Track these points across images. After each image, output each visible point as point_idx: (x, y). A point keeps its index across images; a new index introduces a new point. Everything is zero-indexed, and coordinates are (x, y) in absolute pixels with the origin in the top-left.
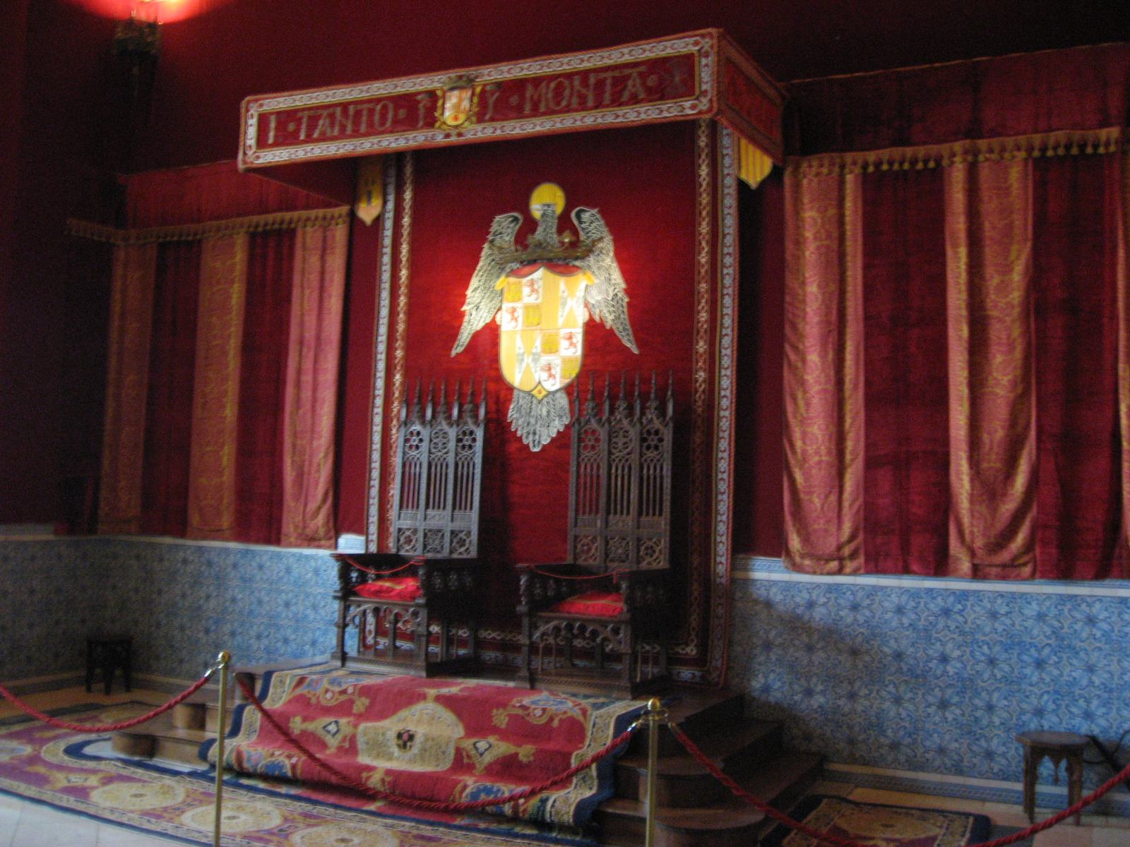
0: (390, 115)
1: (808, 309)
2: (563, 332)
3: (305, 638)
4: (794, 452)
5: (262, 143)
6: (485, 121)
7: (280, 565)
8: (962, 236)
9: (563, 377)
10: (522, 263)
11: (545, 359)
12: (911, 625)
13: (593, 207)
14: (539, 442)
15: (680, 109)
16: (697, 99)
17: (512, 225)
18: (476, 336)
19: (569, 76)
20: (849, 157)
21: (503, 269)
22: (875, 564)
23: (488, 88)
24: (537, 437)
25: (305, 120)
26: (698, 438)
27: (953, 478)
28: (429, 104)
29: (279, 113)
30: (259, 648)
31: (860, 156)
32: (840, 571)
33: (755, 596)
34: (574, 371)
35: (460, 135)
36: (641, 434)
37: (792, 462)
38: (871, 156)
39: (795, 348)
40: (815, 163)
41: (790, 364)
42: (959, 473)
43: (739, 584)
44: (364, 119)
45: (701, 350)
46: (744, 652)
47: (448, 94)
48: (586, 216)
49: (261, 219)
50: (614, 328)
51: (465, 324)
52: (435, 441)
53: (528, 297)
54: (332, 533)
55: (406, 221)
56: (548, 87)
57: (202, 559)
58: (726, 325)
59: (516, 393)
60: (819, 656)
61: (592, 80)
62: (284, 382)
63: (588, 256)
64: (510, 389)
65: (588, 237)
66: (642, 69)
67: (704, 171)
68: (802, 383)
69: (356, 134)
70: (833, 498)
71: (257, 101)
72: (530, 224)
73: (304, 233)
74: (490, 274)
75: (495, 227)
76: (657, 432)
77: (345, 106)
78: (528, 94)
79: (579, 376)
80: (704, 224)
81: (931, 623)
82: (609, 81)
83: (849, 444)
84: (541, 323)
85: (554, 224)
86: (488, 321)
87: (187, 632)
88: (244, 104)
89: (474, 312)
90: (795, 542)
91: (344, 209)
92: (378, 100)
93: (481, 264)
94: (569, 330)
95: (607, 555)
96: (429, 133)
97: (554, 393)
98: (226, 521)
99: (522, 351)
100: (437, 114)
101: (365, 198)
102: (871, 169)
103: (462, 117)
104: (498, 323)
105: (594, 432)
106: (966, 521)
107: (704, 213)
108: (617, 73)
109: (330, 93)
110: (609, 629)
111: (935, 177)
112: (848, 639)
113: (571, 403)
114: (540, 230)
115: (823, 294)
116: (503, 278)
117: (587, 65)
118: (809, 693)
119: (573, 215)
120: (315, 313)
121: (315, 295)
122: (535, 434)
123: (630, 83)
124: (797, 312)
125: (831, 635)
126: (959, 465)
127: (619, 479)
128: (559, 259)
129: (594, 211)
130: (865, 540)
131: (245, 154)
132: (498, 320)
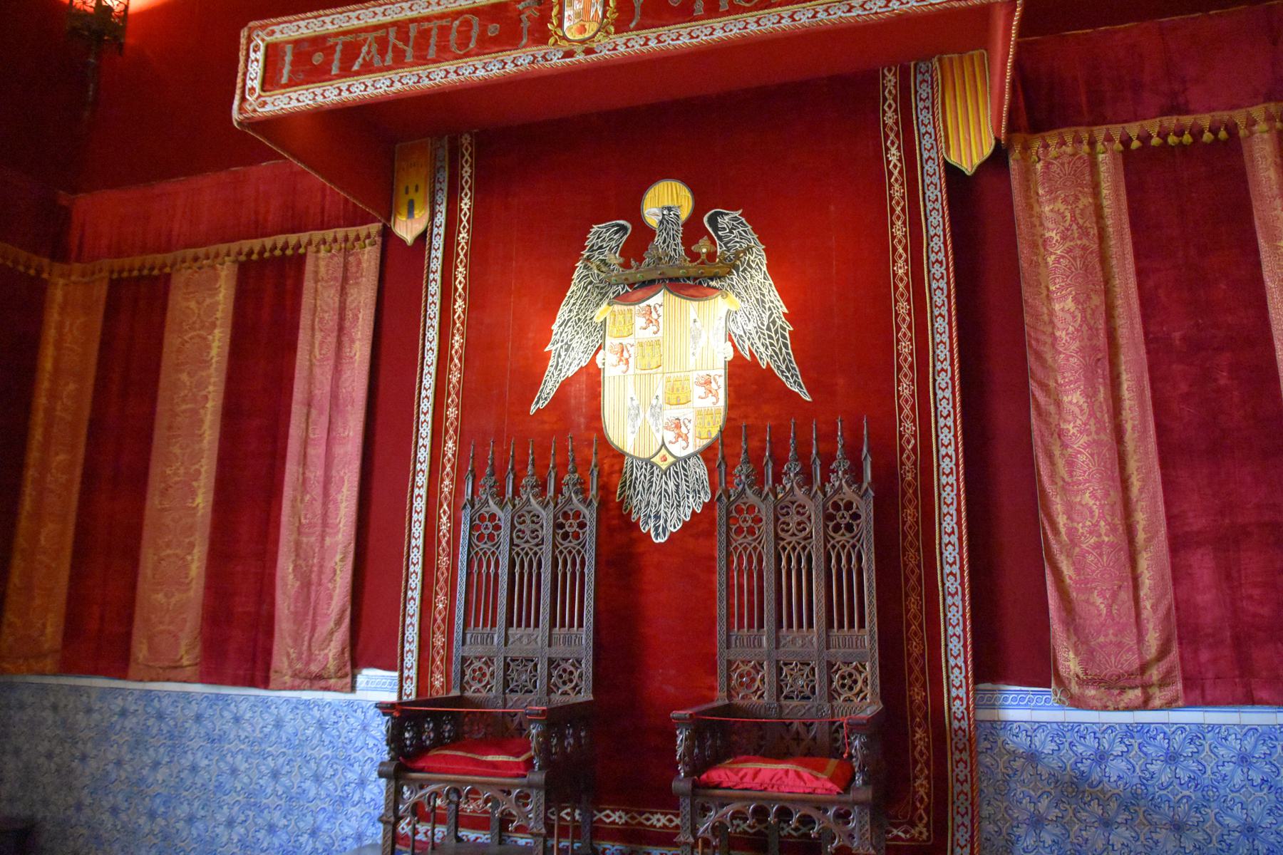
0: (475, 33)
1: (1058, 334)
3: (301, 824)
4: (1056, 532)
5: (269, 82)
7: (266, 716)
10: (631, 286)
11: (671, 413)
14: (664, 529)
20: (1100, 132)
24: (662, 522)
26: (910, 514)
30: (230, 839)
31: (1116, 130)
32: (1145, 705)
33: (1011, 747)
35: (589, 51)
36: (825, 509)
37: (1055, 547)
38: (1134, 129)
39: (1044, 386)
40: (1053, 142)
41: (1038, 406)
45: (906, 393)
46: (999, 833)
48: (724, 221)
49: (256, 244)
54: (348, 668)
55: (463, 236)
57: (149, 709)
59: (627, 460)
62: (284, 457)
63: (730, 273)
64: (620, 455)
67: (894, 155)
68: (1061, 434)
69: (421, 60)
70: (1125, 596)
71: (263, 28)
72: (641, 238)
73: (317, 259)
74: (586, 301)
75: (591, 239)
76: (849, 505)
83: (1141, 518)
84: (664, 365)
86: (583, 364)
87: (123, 816)
88: (244, 33)
89: (563, 354)
90: (1069, 662)
91: (374, 228)
94: (703, 373)
95: (780, 690)
96: (539, 51)
97: (686, 459)
98: (188, 654)
99: (635, 403)
101: (404, 210)
103: (592, 28)
104: (600, 366)
105: (751, 509)
110: (831, 813)
112: (1165, 806)
114: (658, 240)
115: (1084, 311)
116: (604, 305)
119: (705, 219)
120: (332, 362)
121: (332, 339)
122: (657, 517)
124: (1043, 338)
125: (1136, 803)
128: (689, 278)
129: (737, 214)
130: (1182, 658)
131: (243, 99)
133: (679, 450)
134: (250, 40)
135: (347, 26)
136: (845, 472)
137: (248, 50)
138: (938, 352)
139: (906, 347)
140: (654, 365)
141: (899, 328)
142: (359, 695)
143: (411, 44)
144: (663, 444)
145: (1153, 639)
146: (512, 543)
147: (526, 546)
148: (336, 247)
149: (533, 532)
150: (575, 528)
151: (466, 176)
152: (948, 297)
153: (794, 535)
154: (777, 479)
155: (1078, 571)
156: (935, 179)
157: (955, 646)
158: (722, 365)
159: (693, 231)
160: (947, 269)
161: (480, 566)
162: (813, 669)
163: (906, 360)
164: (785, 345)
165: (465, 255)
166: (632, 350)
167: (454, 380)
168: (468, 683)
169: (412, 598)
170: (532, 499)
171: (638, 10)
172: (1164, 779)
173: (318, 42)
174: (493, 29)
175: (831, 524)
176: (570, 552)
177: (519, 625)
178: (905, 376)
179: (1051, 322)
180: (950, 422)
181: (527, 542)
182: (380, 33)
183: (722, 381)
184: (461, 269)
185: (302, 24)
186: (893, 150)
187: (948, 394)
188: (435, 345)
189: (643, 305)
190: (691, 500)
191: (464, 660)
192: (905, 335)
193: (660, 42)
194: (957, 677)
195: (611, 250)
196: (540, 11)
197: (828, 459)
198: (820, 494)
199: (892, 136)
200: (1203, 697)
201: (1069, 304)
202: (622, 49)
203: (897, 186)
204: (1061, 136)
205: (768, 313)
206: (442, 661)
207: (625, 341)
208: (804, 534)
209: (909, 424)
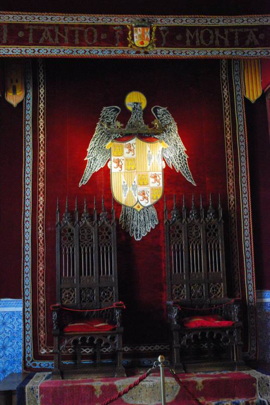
0: (96, 35)
9: (152, 198)
11: (140, 189)
13: (165, 107)
18: (95, 174)
19: (213, 28)
21: (109, 138)
23: (161, 29)
25: (31, 31)
28: (122, 33)
29: (9, 25)
34: (159, 196)
43: (262, 305)
44: (77, 36)
45: (231, 184)
47: (134, 29)
48: (161, 111)
50: (181, 172)
51: (87, 168)
53: (126, 154)
55: (42, 106)
56: (199, 33)
58: (243, 171)
59: (123, 207)
61: (226, 32)
63: (163, 133)
64: (119, 205)
65: (162, 123)
66: (255, 30)
67: (225, 92)
69: (72, 43)
75: (103, 113)
77: (61, 27)
78: (187, 35)
82: (236, 34)
84: (138, 170)
85: (140, 113)
89: (93, 162)
92: (87, 26)
93: (96, 134)
94: (154, 173)
95: (191, 295)
96: (126, 49)
97: (148, 207)
99: (125, 184)
100: (129, 39)
101: (11, 90)
103: (146, 43)
108: (241, 30)
109: (49, 17)
110: (227, 332)
113: (158, 213)
114: (133, 116)
116: (110, 142)
117: (221, 24)
119: (152, 110)
122: (137, 230)
123: (249, 37)
129: (165, 109)
133: (145, 203)
135: (34, 22)
136: (213, 214)
138: (242, 169)
139: (231, 167)
140: (133, 169)
141: (228, 160)
143: (66, 35)
144: (138, 201)
146: (79, 241)
147: (86, 242)
149: (88, 236)
150: (107, 234)
151: (42, 78)
152: (246, 149)
153: (194, 237)
154: (188, 216)
156: (241, 103)
157: (250, 276)
158: (161, 170)
159: (148, 116)
162: (202, 286)
163: (231, 172)
164: (186, 163)
165: (43, 114)
166: (123, 162)
167: (41, 170)
168: (63, 299)
169: (27, 266)
170: (88, 223)
171: (164, 39)
173: (20, 26)
174: (104, 36)
176: (86, 245)
178: (231, 178)
180: (246, 195)
181: (86, 240)
182: (50, 28)
183: (161, 177)
184: (41, 120)
186: (225, 90)
187: (246, 185)
188: (31, 154)
189: (127, 143)
190: (150, 223)
192: (230, 162)
193: (174, 54)
194: (251, 288)
195: (112, 118)
196: (123, 31)
197: (206, 208)
198: (204, 222)
199: (225, 84)
202: (159, 54)
203: (227, 104)
205: (179, 151)
206: (43, 292)
207: (120, 158)
208: (90, 240)
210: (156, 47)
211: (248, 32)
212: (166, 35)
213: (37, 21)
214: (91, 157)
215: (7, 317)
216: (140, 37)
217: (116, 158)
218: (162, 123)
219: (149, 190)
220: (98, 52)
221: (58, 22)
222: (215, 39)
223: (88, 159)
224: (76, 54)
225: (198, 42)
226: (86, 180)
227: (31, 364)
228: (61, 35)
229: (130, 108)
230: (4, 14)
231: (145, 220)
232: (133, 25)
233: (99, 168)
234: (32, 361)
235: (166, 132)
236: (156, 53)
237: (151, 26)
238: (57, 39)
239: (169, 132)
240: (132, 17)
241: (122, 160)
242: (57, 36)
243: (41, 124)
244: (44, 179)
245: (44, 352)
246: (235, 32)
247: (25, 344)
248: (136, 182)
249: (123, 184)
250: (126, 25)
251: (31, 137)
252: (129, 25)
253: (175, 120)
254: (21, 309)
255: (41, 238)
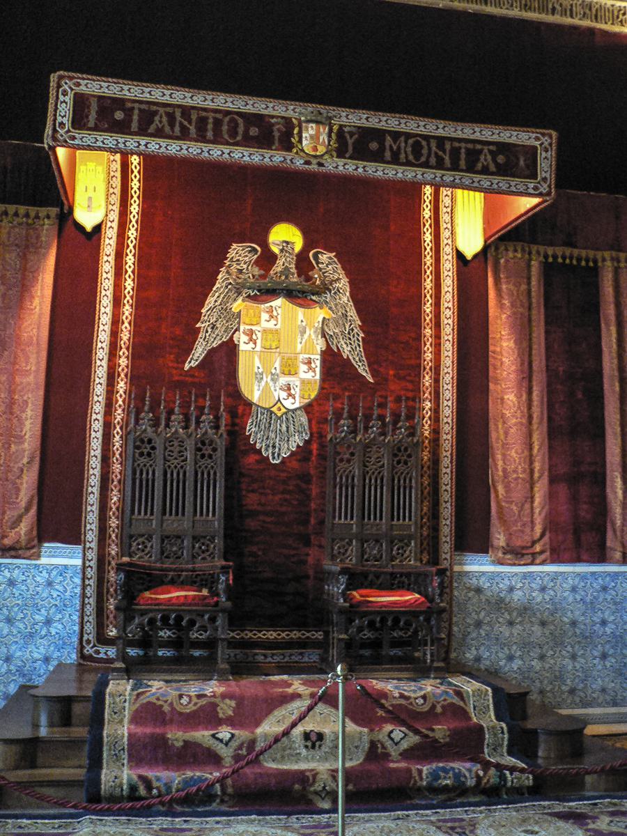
0: (241, 130)
1: (504, 359)
2: (301, 357)
4: (497, 470)
6: (345, 158)
8: (613, 318)
10: (259, 291)
11: (283, 380)
12: (581, 600)
14: (279, 455)
15: (525, 187)
16: (539, 183)
17: (250, 255)
18: (212, 352)
19: (427, 138)
20: (534, 248)
21: (239, 294)
22: (556, 558)
23: (346, 129)
24: (277, 450)
25: (136, 112)
27: (608, 490)
29: (100, 98)
31: (542, 249)
32: (532, 563)
33: (468, 585)
38: (550, 251)
40: (511, 249)
42: (614, 488)
44: (210, 126)
45: (427, 384)
47: (304, 125)
50: (351, 358)
51: (200, 340)
52: (169, 448)
53: (265, 323)
54: (36, 542)
55: (132, 233)
60: (517, 629)
61: (448, 146)
64: (249, 404)
66: (491, 147)
69: (201, 138)
70: (527, 506)
71: (71, 78)
72: (267, 259)
75: (232, 254)
77: (186, 111)
78: (387, 144)
79: (316, 399)
80: (428, 281)
81: (594, 597)
82: (463, 151)
83: (537, 466)
86: (224, 340)
88: (53, 78)
89: (209, 330)
90: (499, 539)
92: (227, 113)
93: (217, 285)
94: (307, 356)
96: (289, 156)
99: (260, 370)
102: (550, 260)
103: (321, 150)
104: (236, 342)
106: (619, 523)
107: (428, 272)
108: (470, 146)
109: (167, 92)
111: (594, 272)
112: (538, 613)
113: (310, 421)
114: (280, 262)
115: (519, 349)
116: (240, 299)
117: (441, 133)
118: (511, 658)
119: (311, 254)
122: (274, 447)
123: (482, 157)
126: (613, 482)
127: (373, 488)
130: (550, 538)
131: (55, 130)
132: (234, 339)
133: (289, 404)
134: (59, 86)
137: (58, 92)
140: (274, 347)
142: (44, 561)
145: (538, 530)
148: (19, 220)
155: (507, 492)
158: (319, 352)
159: (303, 263)
160: (453, 313)
161: (141, 474)
164: (359, 345)
166: (259, 335)
169: (92, 492)
172: (539, 600)
173: (119, 103)
174: (254, 131)
175: (396, 459)
177: (171, 514)
178: (427, 373)
179: (501, 352)
182: (169, 110)
183: (318, 363)
185: (105, 85)
188: (109, 310)
190: (297, 437)
191: (131, 537)
193: (365, 171)
200: (558, 558)
201: (512, 344)
202: (341, 168)
203: (428, 257)
204: (515, 246)
207: (254, 328)
209: (429, 403)
210: (338, 157)
211: (481, 151)
212: (353, 140)
213: (146, 96)
214: (208, 323)
215: (54, 573)
216: (313, 139)
217: (249, 327)
218: (325, 277)
219: (298, 383)
220: (244, 156)
221: (184, 102)
222: (429, 155)
223: (203, 325)
224: (207, 155)
225: (403, 156)
226: (197, 360)
227: (91, 651)
228: (186, 123)
229: (276, 250)
230: (94, 81)
231: (287, 431)
232: (303, 119)
233: (220, 342)
234: (94, 646)
235: (330, 293)
236: (336, 167)
237: (331, 123)
238: (177, 129)
239: (335, 293)
240: (301, 106)
241: (257, 332)
242: (177, 124)
243: (130, 263)
244: (128, 351)
245: (113, 632)
246: (460, 148)
247: (83, 618)
248: (278, 369)
249: (256, 370)
250: (290, 119)
251: (112, 281)
252: (295, 119)
253: (347, 275)
254: (79, 562)
255: (117, 449)
